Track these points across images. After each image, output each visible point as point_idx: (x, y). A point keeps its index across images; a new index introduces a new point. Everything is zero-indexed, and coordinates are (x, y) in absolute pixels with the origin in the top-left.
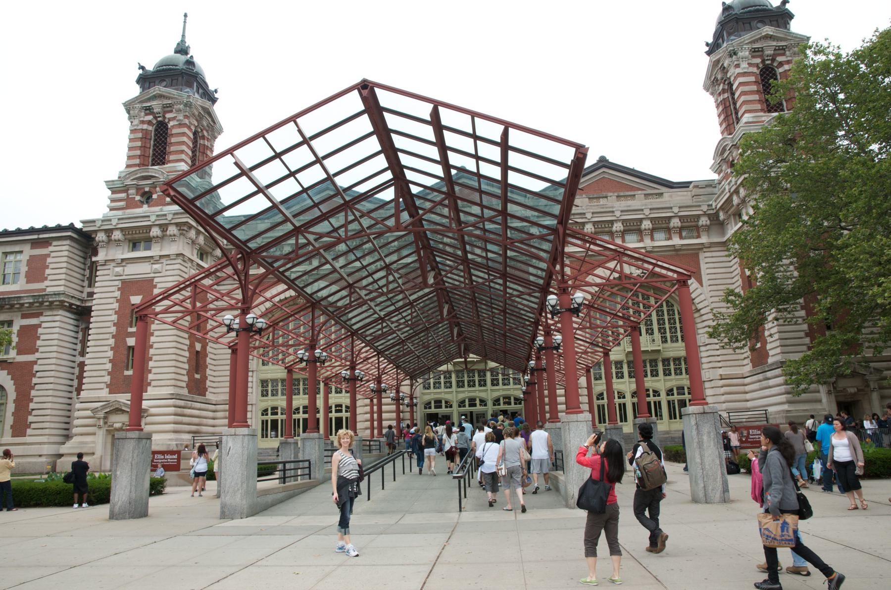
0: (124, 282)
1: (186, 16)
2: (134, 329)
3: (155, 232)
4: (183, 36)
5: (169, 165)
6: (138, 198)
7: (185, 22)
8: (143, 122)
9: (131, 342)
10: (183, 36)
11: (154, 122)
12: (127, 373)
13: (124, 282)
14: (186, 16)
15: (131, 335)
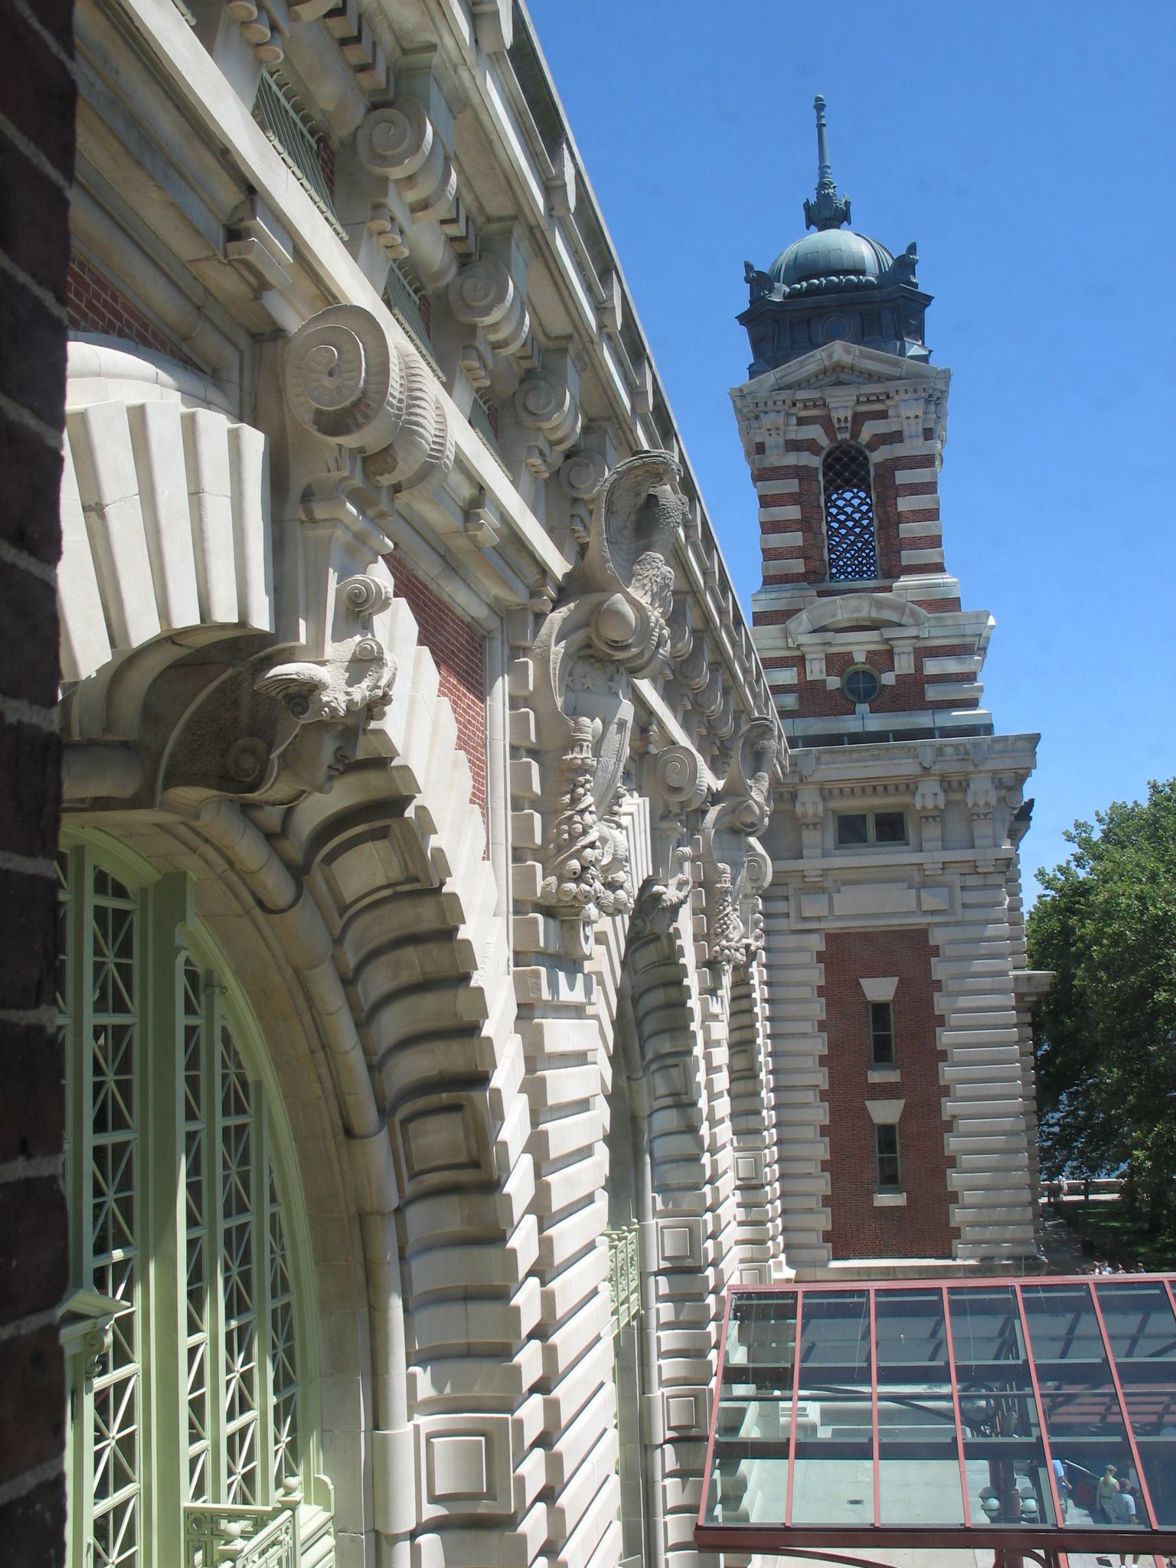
0: (832, 938)
1: (820, 106)
2: (893, 1076)
3: (929, 796)
4: (823, 168)
5: (906, 581)
6: (834, 682)
7: (820, 126)
8: (793, 446)
9: (885, 1112)
10: (823, 168)
11: (824, 442)
12: (885, 1200)
13: (832, 938)
14: (820, 106)
15: (886, 1092)
